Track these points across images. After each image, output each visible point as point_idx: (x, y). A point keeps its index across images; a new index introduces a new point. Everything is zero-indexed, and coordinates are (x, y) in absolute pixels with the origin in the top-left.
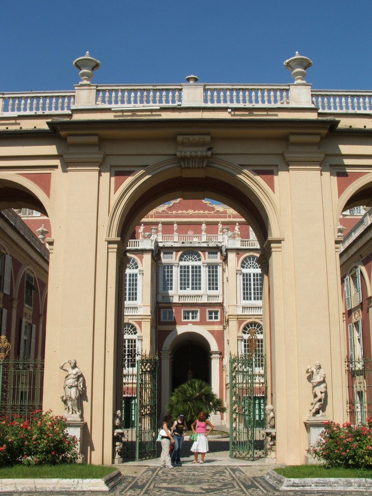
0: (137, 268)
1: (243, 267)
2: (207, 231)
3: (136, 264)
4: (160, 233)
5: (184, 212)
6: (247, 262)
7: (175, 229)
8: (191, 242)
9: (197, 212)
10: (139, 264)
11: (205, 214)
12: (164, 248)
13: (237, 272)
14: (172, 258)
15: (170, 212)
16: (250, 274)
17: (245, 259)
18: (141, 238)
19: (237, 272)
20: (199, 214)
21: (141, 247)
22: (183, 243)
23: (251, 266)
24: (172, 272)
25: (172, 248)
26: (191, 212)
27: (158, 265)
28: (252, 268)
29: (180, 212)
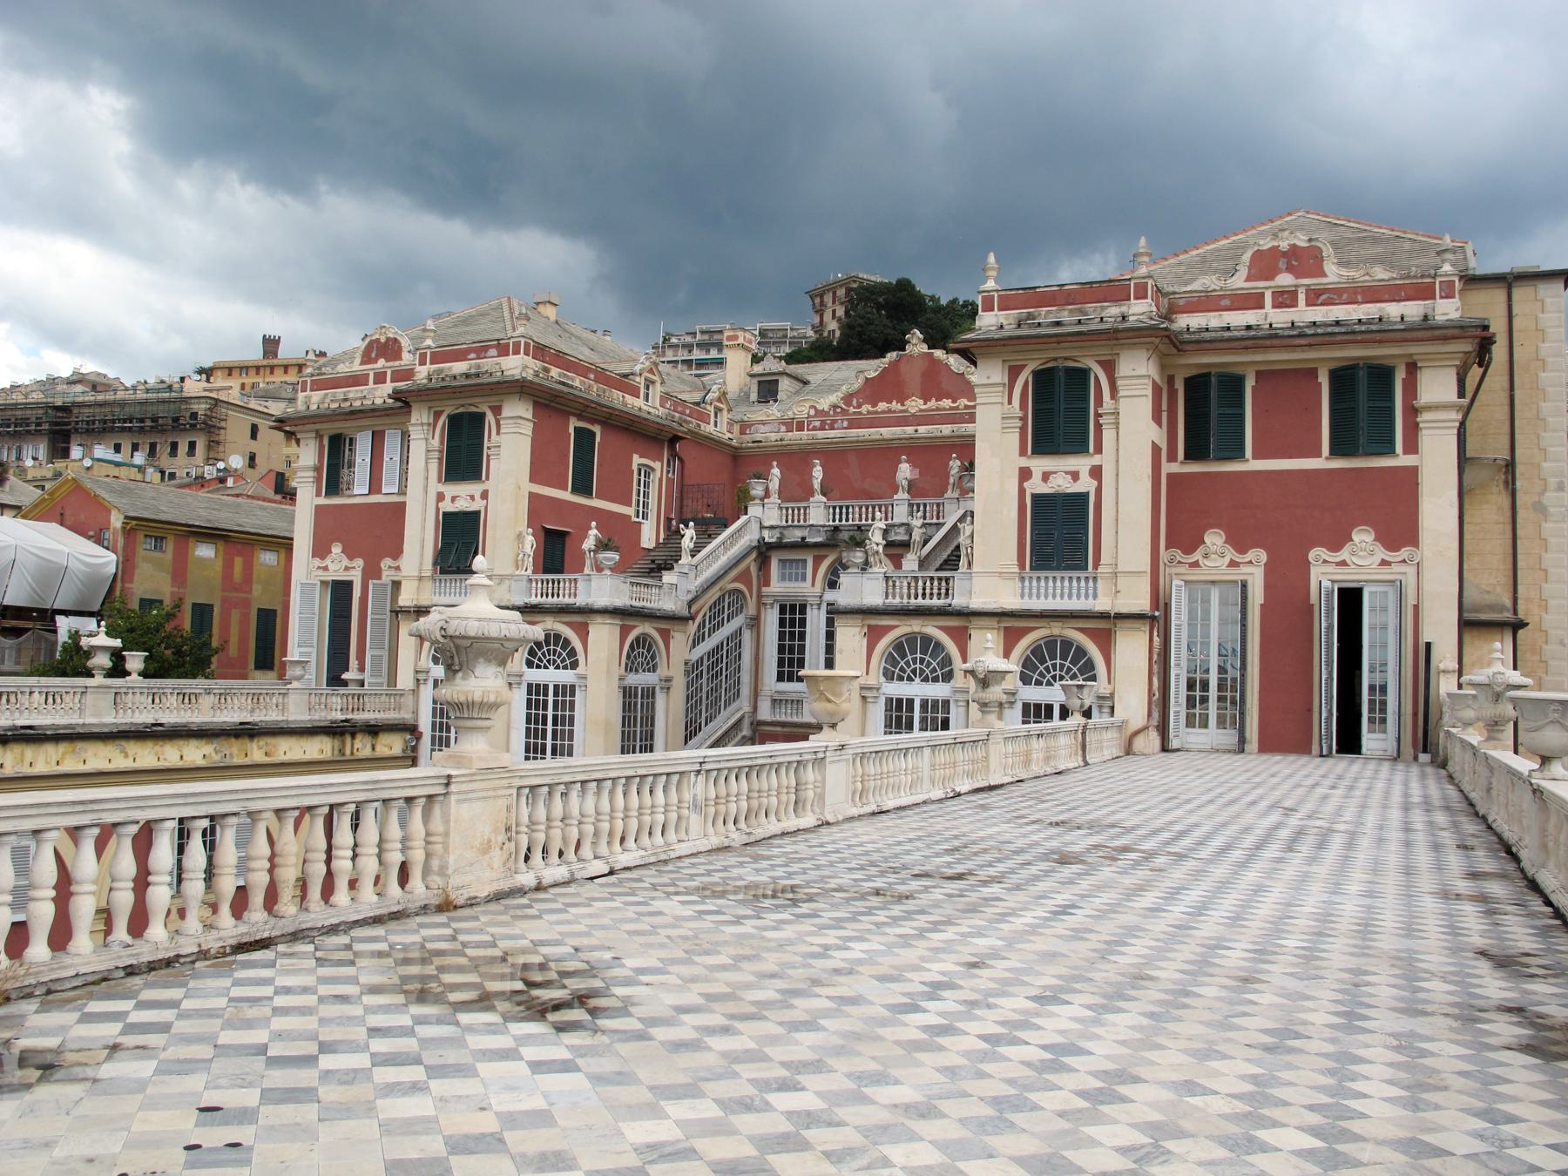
0: (574, 665)
1: (889, 676)
2: (912, 488)
3: (573, 653)
4: (774, 499)
5: (895, 405)
6: (913, 652)
7: (817, 485)
8: (859, 527)
9: (932, 404)
10: (581, 657)
11: (957, 408)
12: (780, 546)
13: (867, 694)
14: (804, 579)
15: (852, 410)
16: (911, 702)
17: (898, 647)
18: (587, 571)
19: (867, 694)
20: (938, 409)
21: (581, 600)
22: (836, 529)
23: (914, 672)
24: (803, 623)
25: (802, 545)
26: (915, 405)
27: (764, 600)
28: (917, 680)
29: (882, 406)
